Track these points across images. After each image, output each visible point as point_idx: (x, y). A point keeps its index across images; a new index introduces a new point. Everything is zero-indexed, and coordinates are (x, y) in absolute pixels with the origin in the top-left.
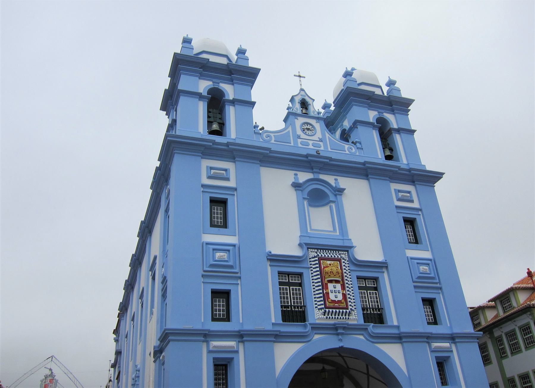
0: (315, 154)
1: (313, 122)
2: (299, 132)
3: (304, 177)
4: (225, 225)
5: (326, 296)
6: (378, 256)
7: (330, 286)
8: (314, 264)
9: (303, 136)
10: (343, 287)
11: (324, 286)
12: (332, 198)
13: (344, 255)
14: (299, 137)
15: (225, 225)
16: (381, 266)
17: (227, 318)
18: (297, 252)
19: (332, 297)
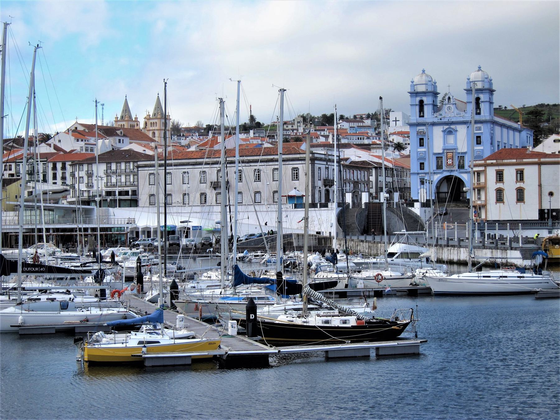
0: (447, 121)
1: (451, 106)
2: (446, 110)
3: (446, 127)
4: (423, 146)
5: (447, 163)
6: (465, 150)
7: (449, 160)
8: (445, 154)
9: (448, 112)
10: (452, 160)
11: (447, 160)
12: (454, 133)
13: (454, 151)
14: (446, 113)
15: (423, 146)
16: (465, 153)
17: (423, 169)
18: (441, 151)
19: (449, 163)
